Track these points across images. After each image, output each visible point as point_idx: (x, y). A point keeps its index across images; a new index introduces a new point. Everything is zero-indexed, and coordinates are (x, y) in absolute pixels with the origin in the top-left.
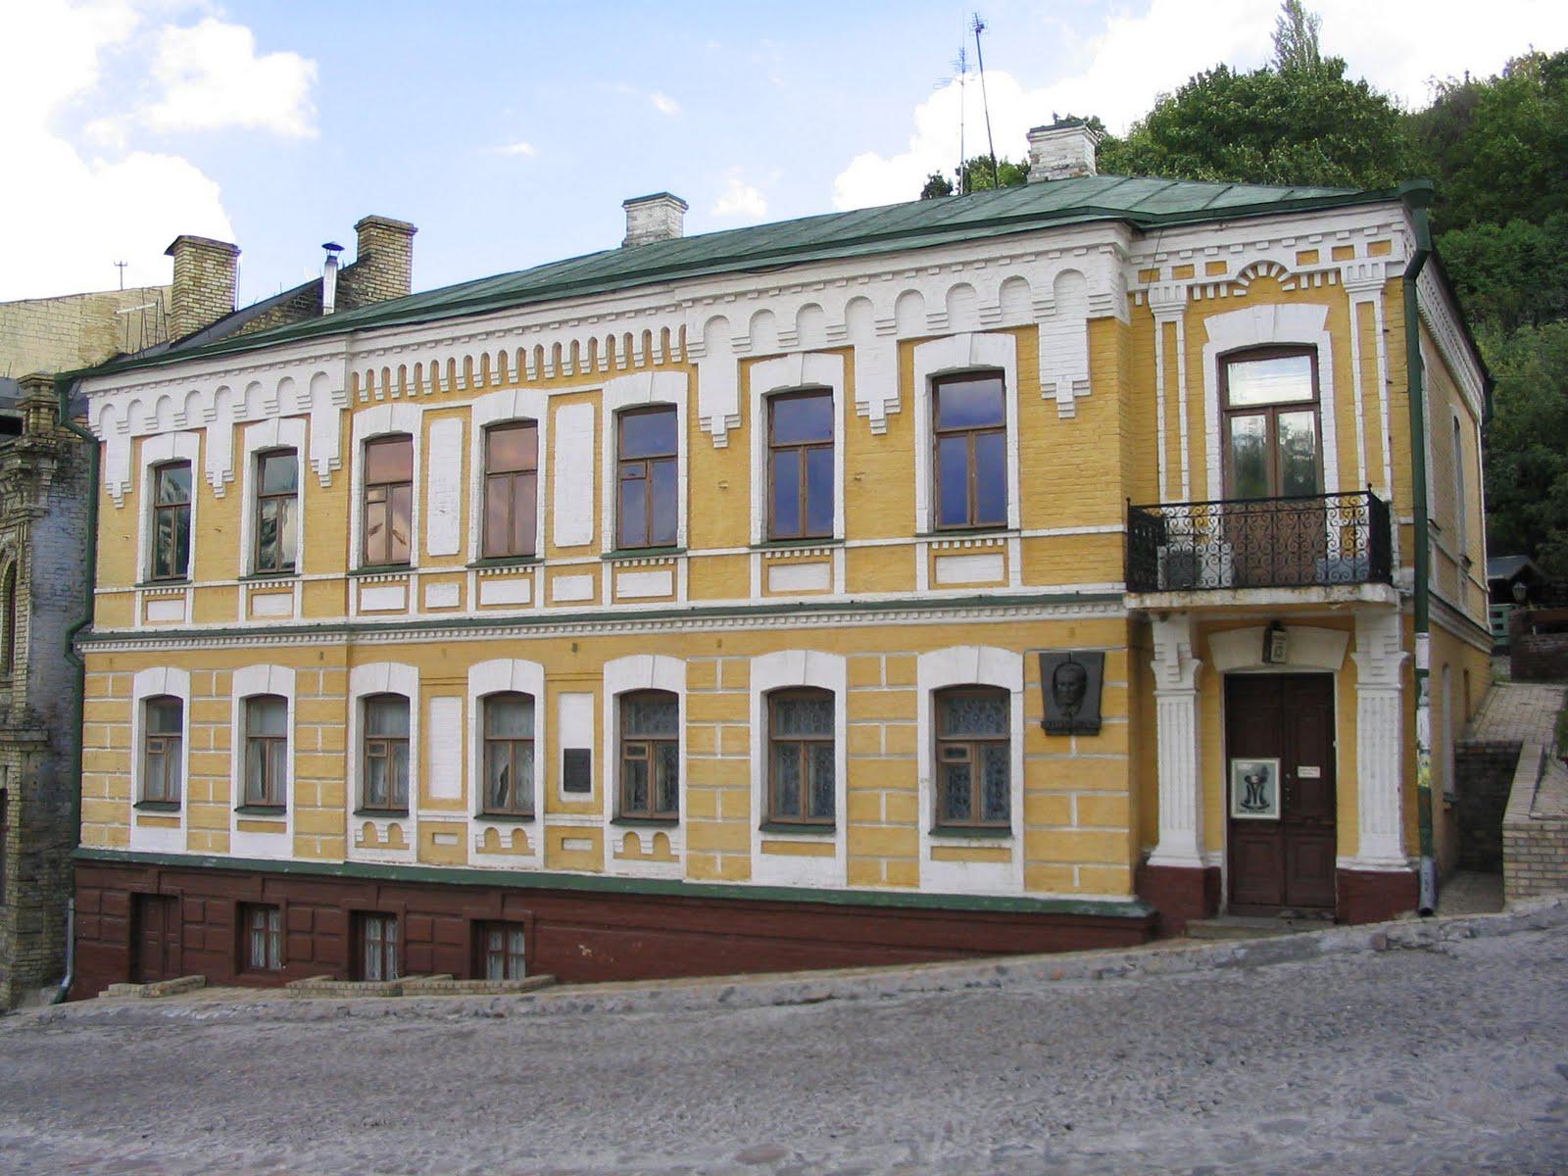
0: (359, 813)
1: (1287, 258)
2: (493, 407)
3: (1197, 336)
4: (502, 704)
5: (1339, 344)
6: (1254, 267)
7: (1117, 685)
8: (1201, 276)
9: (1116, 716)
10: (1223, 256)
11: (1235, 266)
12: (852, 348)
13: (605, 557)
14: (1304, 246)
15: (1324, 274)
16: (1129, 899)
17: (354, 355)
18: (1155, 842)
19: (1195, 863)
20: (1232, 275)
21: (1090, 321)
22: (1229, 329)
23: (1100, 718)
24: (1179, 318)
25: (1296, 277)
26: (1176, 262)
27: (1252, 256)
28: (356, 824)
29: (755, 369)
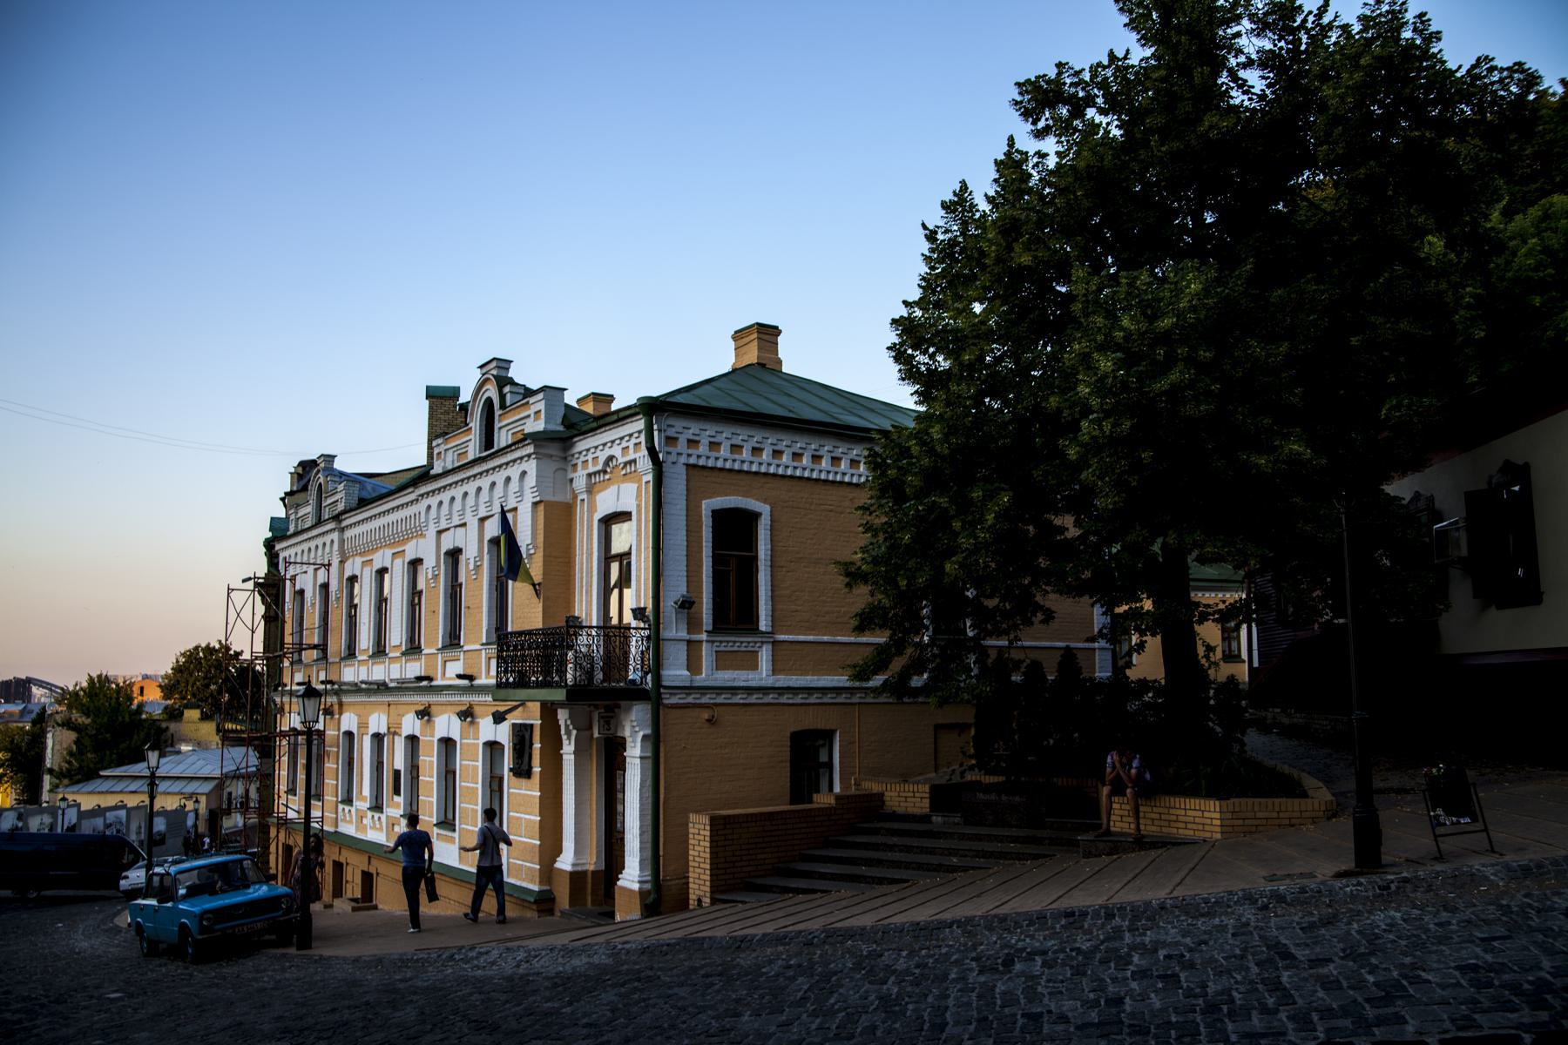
0: (343, 802)
1: (616, 450)
2: (381, 558)
3: (592, 508)
4: (378, 738)
5: (639, 512)
6: (611, 458)
7: (537, 745)
8: (591, 469)
9: (537, 769)
10: (598, 453)
11: (603, 456)
12: (464, 525)
13: (403, 654)
14: (624, 444)
15: (634, 461)
16: (536, 888)
17: (342, 530)
18: (558, 850)
19: (568, 868)
20: (599, 467)
21: (535, 504)
22: (607, 502)
23: (530, 767)
24: (585, 496)
25: (626, 464)
26: (582, 459)
27: (608, 452)
28: (341, 806)
29: (444, 535)
